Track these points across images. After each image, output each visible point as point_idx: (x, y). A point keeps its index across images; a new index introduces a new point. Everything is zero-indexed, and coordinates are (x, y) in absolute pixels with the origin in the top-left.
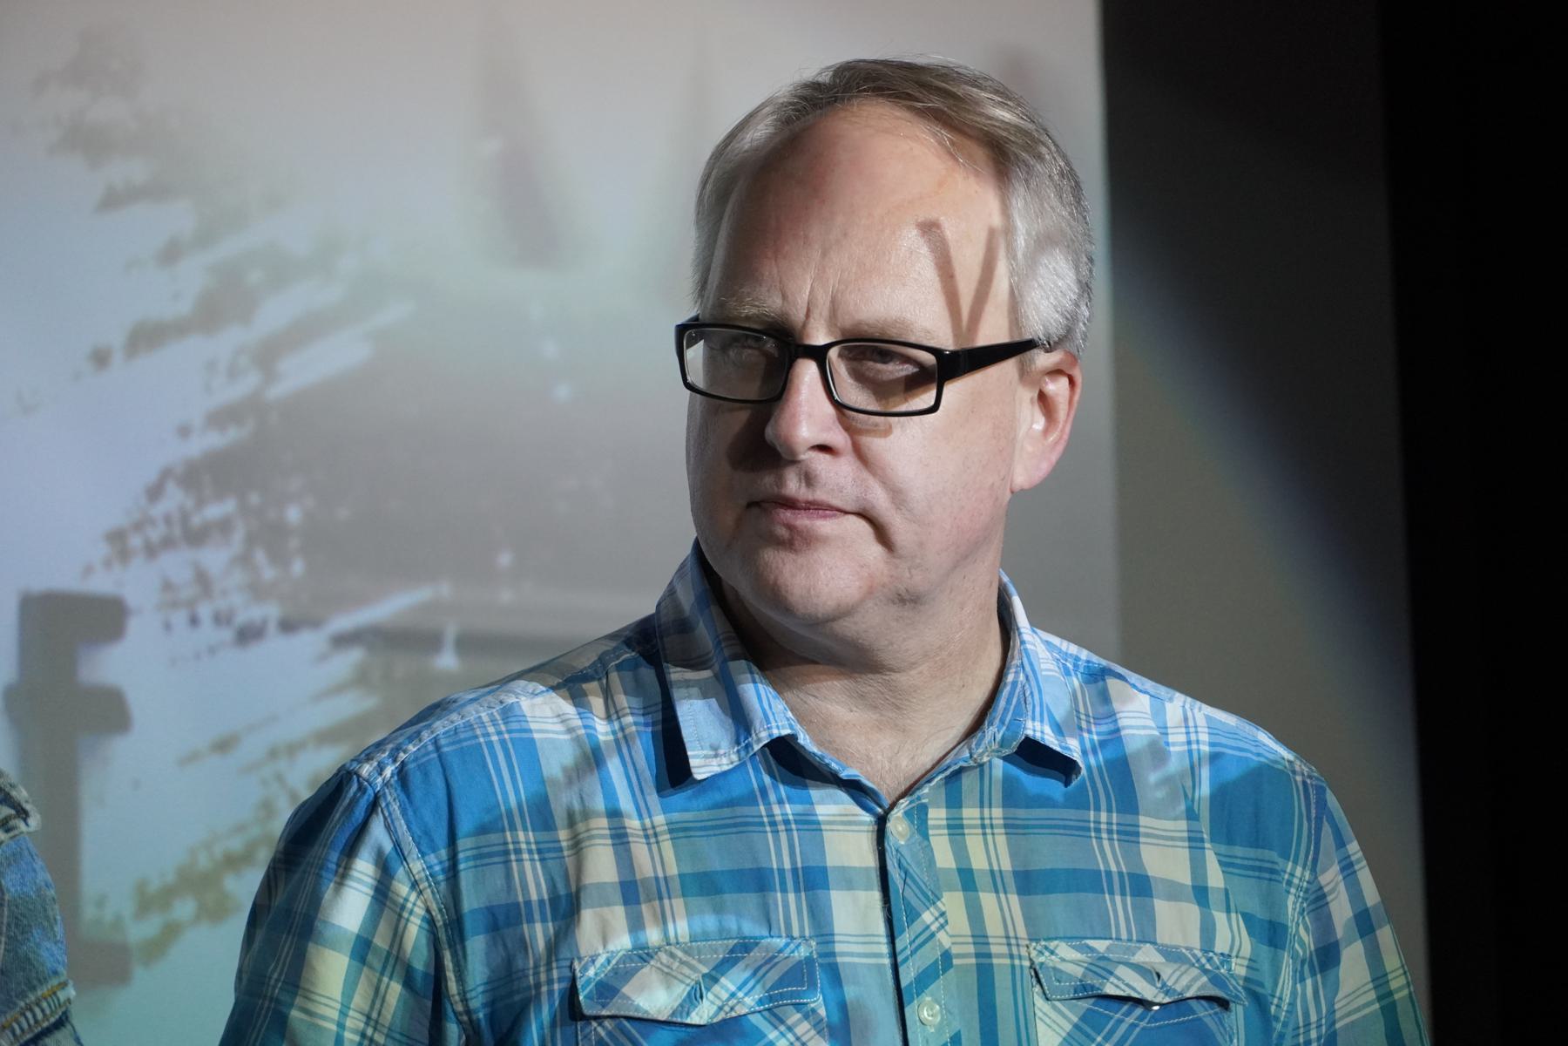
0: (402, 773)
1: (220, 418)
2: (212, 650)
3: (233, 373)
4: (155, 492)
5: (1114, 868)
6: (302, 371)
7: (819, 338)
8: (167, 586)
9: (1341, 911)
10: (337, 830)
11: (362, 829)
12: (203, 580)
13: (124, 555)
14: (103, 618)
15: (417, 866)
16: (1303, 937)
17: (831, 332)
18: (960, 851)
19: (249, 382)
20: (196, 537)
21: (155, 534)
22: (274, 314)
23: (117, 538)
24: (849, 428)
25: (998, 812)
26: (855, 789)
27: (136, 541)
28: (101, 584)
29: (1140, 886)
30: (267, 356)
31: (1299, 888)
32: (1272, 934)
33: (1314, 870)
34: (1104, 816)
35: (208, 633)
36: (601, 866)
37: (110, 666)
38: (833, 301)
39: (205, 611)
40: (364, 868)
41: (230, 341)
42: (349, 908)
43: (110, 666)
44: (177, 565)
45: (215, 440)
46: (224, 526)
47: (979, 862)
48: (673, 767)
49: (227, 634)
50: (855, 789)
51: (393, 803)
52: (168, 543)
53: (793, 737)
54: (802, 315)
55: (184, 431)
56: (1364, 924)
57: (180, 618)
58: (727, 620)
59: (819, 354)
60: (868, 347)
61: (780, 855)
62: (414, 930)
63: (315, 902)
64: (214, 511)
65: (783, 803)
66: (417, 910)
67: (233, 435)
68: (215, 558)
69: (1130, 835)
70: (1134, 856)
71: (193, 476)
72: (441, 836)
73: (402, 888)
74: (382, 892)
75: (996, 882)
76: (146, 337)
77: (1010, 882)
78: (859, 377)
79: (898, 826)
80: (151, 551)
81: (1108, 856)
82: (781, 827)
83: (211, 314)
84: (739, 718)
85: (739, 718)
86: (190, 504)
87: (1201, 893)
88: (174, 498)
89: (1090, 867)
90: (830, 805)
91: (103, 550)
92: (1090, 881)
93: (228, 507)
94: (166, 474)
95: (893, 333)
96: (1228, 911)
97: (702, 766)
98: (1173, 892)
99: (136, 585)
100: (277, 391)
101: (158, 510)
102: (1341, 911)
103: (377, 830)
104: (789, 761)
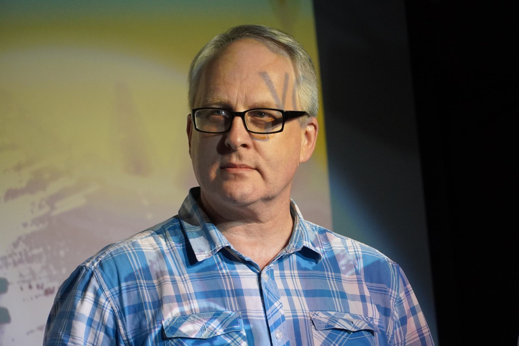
0: (101, 265)
2: (37, 297)
3: (40, 207)
5: (334, 290)
7: (241, 110)
9: (406, 306)
10: (80, 283)
11: (89, 282)
12: (33, 273)
15: (108, 293)
16: (396, 314)
17: (245, 106)
18: (285, 283)
19: (46, 209)
22: (53, 188)
24: (252, 137)
25: (296, 272)
26: (250, 264)
29: (343, 295)
30: (52, 200)
31: (394, 298)
32: (386, 312)
33: (398, 292)
34: (330, 273)
35: (35, 291)
36: (169, 290)
38: (246, 97)
40: (90, 295)
41: (39, 196)
42: (85, 307)
45: (34, 228)
47: (291, 287)
48: (191, 258)
49: (42, 292)
50: (250, 264)
51: (98, 273)
53: (229, 247)
54: (235, 102)
56: (413, 311)
58: (209, 207)
59: (242, 115)
60: (257, 112)
61: (227, 285)
62: (108, 315)
63: (74, 307)
64: (35, 252)
65: (225, 268)
66: (109, 305)
68: (36, 267)
69: (339, 280)
70: (340, 286)
72: (115, 281)
73: (102, 300)
74: (96, 302)
75: (297, 292)
77: (302, 293)
78: (255, 123)
79: (264, 276)
81: (333, 286)
82: (226, 277)
84: (211, 241)
85: (211, 241)
87: (363, 298)
89: (327, 289)
90: (241, 269)
92: (326, 293)
93: (41, 250)
95: (267, 106)
96: (372, 303)
97: (200, 257)
98: (354, 298)
100: (55, 213)
102: (406, 306)
103: (94, 282)
104: (229, 255)
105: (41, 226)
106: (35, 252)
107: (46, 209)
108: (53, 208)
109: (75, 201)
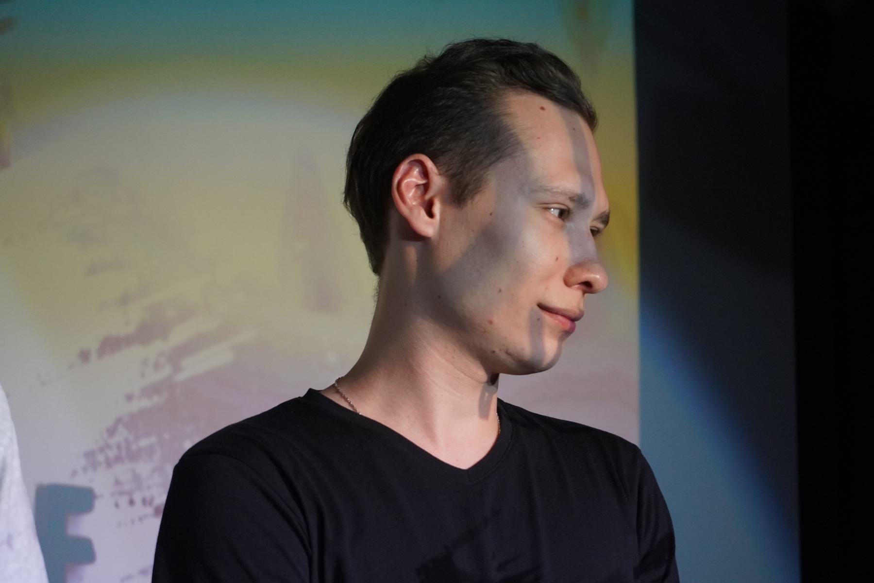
1: (150, 391)
2: (141, 519)
3: (157, 366)
4: (112, 431)
6: (195, 366)
8: (117, 483)
12: (137, 478)
13: (94, 465)
14: (82, 500)
19: (167, 371)
20: (134, 457)
21: (111, 454)
22: (180, 335)
23: (90, 455)
27: (101, 458)
28: (81, 481)
30: (177, 355)
37: (85, 526)
39: (137, 497)
41: (157, 348)
43: (85, 526)
44: (122, 471)
45: (145, 403)
46: (150, 451)
52: (118, 459)
55: (129, 398)
57: (124, 501)
64: (144, 442)
67: (156, 400)
71: (133, 422)
76: (111, 345)
80: (109, 464)
83: (146, 333)
86: (131, 438)
88: (122, 434)
91: (83, 462)
93: (153, 440)
94: (119, 421)
99: (100, 482)
100: (180, 377)
101: (114, 441)
105: (156, 400)
106: (144, 442)
107: (167, 371)
108: (177, 369)
109: (216, 357)
